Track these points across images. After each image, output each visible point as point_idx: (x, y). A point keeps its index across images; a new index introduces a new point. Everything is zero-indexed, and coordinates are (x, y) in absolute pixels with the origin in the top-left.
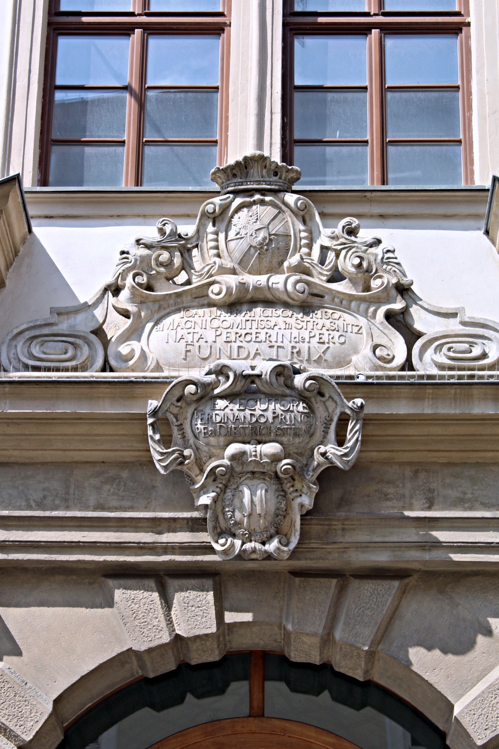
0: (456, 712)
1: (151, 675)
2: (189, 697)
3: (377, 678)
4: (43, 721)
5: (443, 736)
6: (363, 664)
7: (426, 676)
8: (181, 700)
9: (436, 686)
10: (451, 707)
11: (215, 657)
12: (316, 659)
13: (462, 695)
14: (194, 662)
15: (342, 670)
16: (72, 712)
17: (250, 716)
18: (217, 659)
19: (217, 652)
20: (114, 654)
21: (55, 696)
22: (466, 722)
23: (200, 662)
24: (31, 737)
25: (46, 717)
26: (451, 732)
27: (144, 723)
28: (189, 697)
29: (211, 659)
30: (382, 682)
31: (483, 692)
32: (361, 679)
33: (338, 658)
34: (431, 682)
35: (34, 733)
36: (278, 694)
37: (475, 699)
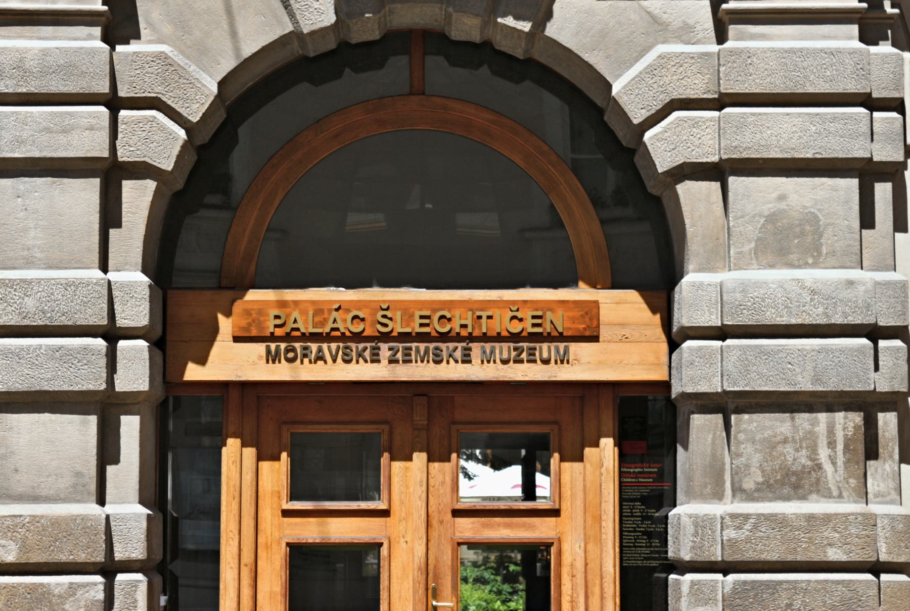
0: (614, 92)
1: (312, 55)
2: (347, 70)
3: (536, 57)
4: (209, 102)
5: (601, 112)
6: (523, 44)
7: (586, 57)
8: (338, 75)
9: (595, 66)
10: (609, 86)
11: (376, 35)
12: (476, 37)
13: (620, 76)
14: (354, 42)
15: (503, 49)
16: (234, 93)
17: (411, 94)
18: (378, 38)
19: (377, 33)
20: (276, 37)
21: (219, 78)
22: (624, 101)
23: (360, 41)
24: (198, 119)
25: (212, 98)
26: (609, 109)
27: (302, 98)
28: (347, 70)
29: (371, 38)
30: (542, 60)
31: (641, 73)
32: (521, 58)
33: (498, 38)
34: (591, 62)
35: (200, 115)
36: (438, 69)
37: (633, 79)
